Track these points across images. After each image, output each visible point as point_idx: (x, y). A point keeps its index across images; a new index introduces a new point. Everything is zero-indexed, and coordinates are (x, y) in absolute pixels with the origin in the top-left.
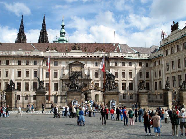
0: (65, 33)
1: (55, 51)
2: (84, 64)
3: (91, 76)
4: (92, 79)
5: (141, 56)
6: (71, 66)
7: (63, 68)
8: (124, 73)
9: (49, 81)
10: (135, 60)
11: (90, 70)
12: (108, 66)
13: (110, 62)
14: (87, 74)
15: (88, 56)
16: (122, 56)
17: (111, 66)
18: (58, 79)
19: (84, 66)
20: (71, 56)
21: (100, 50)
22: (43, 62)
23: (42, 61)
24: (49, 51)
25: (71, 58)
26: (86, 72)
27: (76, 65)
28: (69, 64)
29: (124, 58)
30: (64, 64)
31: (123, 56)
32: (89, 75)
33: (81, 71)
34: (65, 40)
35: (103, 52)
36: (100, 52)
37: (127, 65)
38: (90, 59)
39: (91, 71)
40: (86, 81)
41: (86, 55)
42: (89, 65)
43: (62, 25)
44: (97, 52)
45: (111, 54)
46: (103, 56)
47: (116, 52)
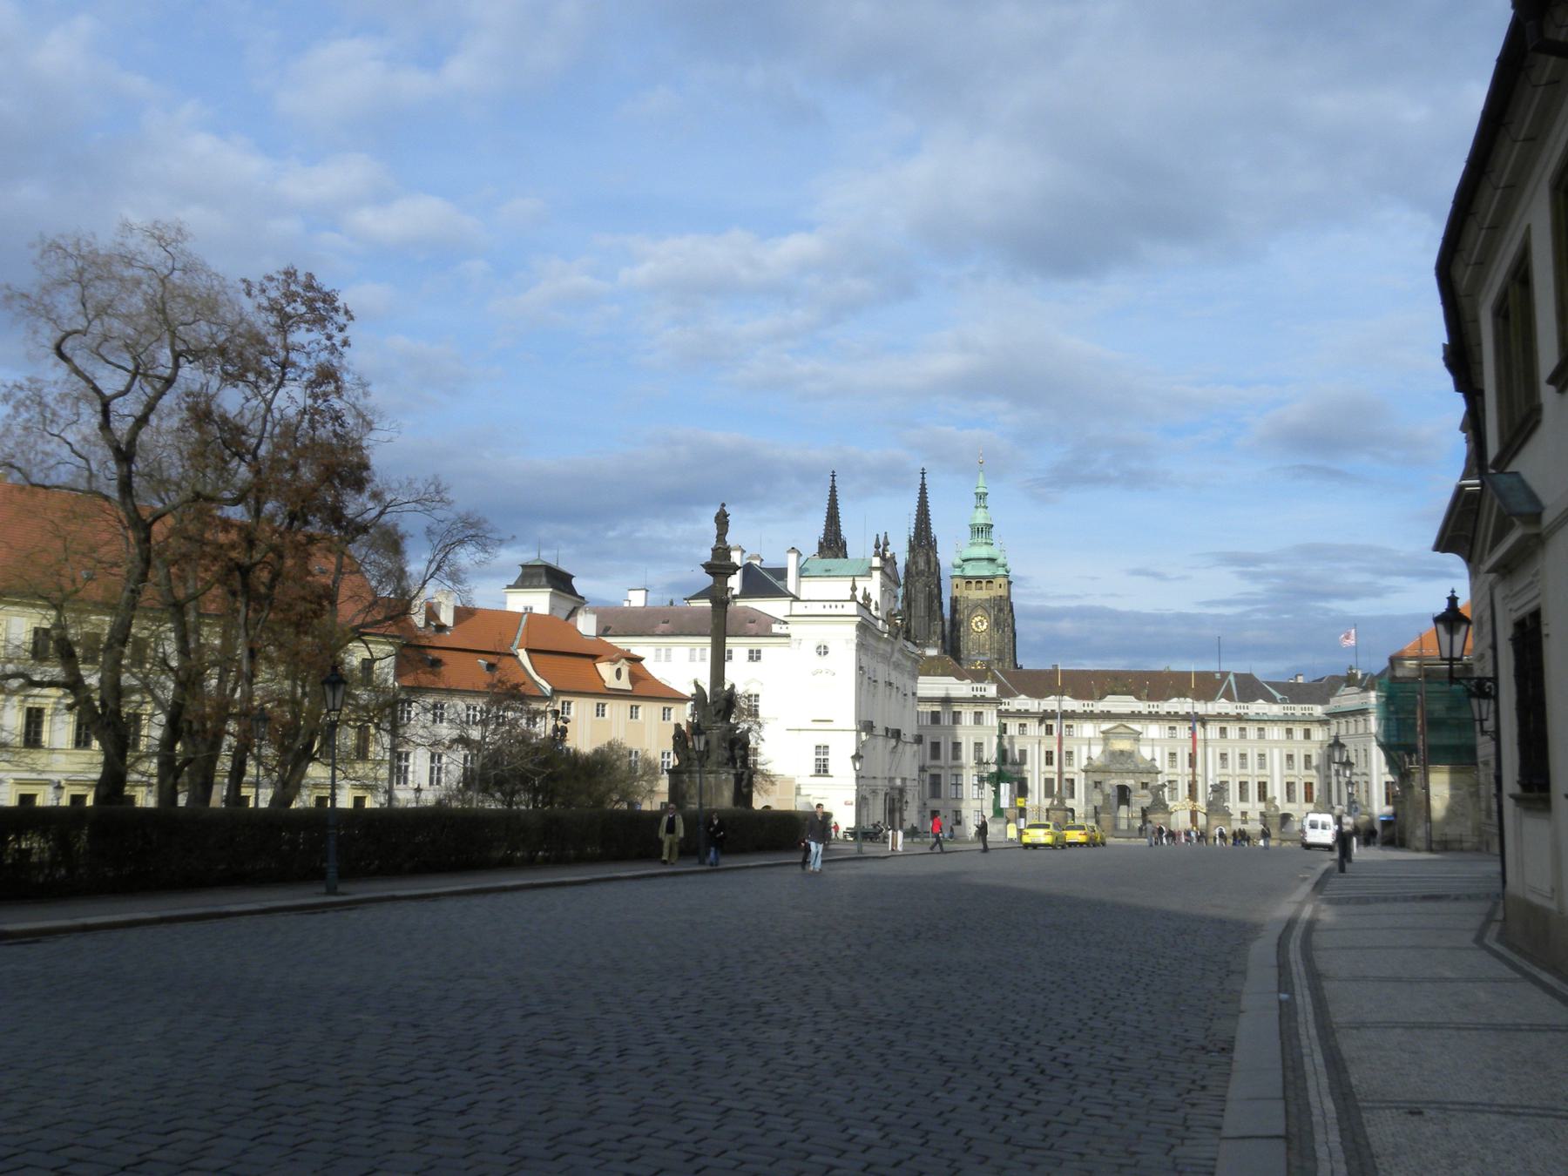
3: (1158, 764)
6: (1106, 734)
7: (1089, 742)
8: (1243, 756)
9: (1061, 773)
10: (1274, 721)
11: (1156, 744)
13: (1208, 727)
14: (1148, 758)
18: (1076, 769)
21: (1181, 694)
25: (1107, 716)
26: (1146, 752)
27: (1119, 736)
30: (1088, 729)
31: (1242, 711)
34: (992, 560)
37: (1252, 732)
38: (1154, 717)
42: (1154, 730)
43: (981, 490)
45: (1210, 705)
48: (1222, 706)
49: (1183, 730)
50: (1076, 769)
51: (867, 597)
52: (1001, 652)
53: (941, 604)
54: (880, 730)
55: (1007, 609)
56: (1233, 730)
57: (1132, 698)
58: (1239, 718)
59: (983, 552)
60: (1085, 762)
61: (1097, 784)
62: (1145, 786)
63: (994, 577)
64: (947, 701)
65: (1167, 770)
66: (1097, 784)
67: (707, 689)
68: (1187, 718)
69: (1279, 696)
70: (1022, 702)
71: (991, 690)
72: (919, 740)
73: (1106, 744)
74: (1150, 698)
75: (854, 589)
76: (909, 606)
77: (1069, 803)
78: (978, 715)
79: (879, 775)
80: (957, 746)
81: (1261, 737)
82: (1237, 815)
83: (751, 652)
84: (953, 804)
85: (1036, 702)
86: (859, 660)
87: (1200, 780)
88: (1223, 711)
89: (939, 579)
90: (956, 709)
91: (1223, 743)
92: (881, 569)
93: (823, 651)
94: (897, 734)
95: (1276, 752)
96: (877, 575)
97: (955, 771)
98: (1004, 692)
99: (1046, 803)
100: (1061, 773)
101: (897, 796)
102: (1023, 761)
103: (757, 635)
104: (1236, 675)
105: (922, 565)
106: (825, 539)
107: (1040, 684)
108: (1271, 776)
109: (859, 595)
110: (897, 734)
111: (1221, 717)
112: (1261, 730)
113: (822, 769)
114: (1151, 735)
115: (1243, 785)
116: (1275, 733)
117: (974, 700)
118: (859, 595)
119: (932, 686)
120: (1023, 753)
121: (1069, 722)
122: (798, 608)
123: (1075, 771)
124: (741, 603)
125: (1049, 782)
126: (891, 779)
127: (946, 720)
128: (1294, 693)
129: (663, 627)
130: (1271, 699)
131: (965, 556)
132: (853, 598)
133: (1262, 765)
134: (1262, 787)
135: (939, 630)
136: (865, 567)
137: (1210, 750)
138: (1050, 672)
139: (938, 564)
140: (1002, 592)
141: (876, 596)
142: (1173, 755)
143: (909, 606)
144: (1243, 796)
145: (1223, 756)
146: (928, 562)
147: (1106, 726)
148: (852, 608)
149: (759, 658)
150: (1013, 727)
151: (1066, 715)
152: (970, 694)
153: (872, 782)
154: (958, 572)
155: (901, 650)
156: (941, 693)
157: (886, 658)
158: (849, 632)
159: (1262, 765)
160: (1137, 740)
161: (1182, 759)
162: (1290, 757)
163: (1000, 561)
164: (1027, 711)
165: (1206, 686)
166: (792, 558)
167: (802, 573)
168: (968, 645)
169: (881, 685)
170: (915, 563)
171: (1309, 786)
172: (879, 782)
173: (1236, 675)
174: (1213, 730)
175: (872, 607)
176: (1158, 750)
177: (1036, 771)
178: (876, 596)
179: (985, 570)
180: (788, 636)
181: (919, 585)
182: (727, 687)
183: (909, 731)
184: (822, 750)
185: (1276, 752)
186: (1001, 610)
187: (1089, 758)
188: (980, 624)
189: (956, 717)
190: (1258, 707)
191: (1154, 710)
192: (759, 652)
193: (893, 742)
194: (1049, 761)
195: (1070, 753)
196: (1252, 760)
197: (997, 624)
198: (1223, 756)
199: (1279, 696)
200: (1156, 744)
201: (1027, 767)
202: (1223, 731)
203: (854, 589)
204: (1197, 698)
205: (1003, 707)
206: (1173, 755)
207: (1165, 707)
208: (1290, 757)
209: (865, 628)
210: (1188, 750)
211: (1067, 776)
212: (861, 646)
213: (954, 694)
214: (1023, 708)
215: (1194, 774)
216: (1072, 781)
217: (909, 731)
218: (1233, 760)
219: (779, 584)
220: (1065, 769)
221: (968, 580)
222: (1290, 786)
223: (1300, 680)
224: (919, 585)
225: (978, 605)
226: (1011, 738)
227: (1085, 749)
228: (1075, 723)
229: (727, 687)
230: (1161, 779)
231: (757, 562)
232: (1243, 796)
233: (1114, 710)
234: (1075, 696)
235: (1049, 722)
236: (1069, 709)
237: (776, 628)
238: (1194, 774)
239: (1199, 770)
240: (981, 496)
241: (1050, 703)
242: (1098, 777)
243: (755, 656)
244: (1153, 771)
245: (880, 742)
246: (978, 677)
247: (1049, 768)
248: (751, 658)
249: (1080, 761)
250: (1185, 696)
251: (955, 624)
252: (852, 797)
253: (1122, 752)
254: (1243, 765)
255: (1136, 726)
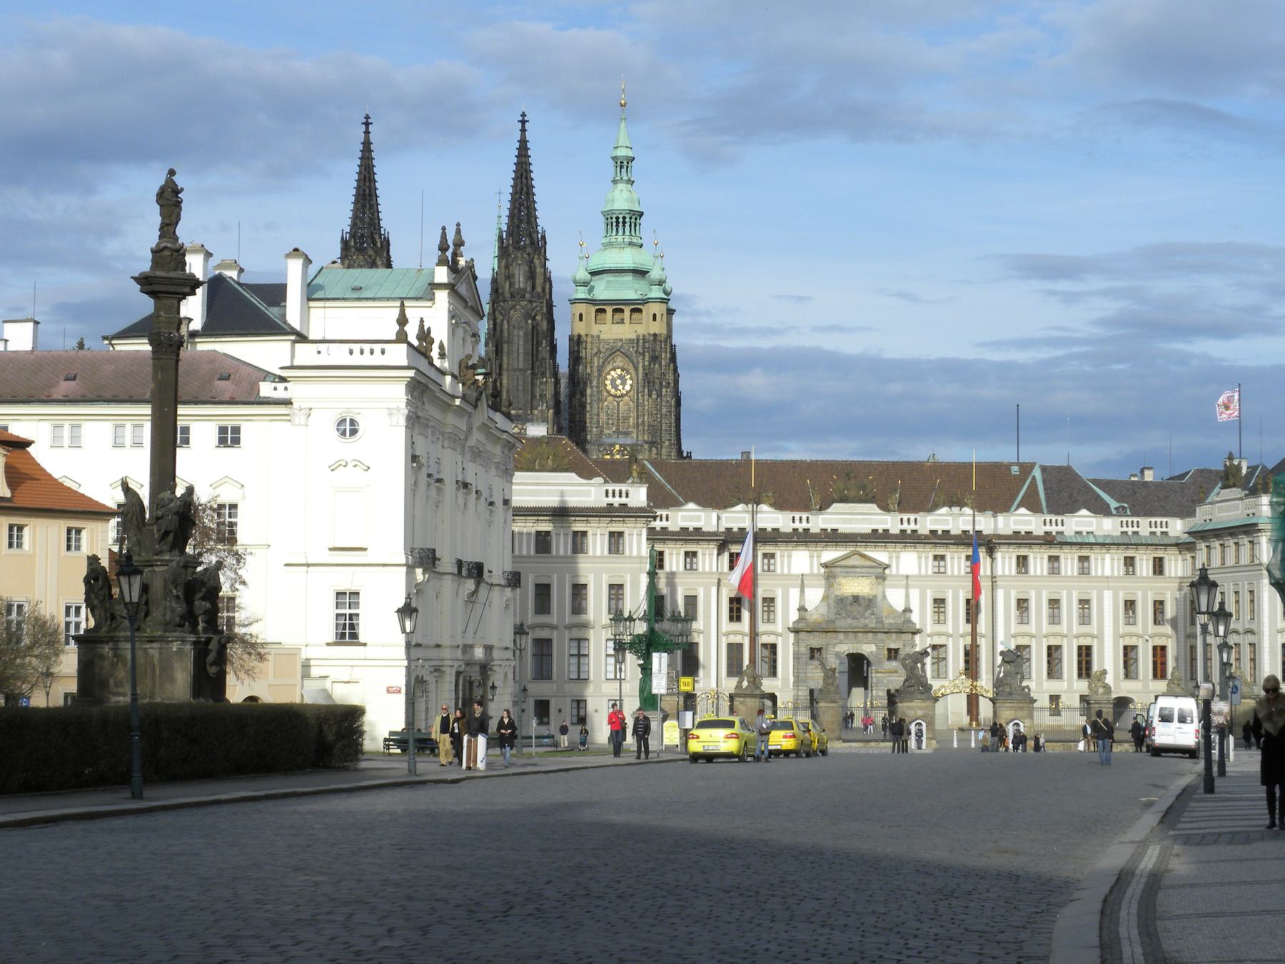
0: (641, 214)
1: (764, 507)
2: (888, 566)
3: (915, 617)
4: (919, 632)
5: (1135, 529)
7: (802, 582)
8: (1054, 603)
9: (754, 635)
10: (1105, 545)
12: (989, 573)
13: (998, 555)
15: (905, 526)
16: (1048, 528)
17: (999, 572)
18: (779, 626)
19: (887, 571)
20: (829, 527)
21: (955, 501)
22: (719, 554)
23: (715, 552)
24: (740, 507)
25: (832, 538)
26: (895, 598)
27: (851, 571)
28: (826, 566)
29: (1059, 539)
30: (800, 561)
31: (1054, 529)
32: (908, 610)
33: (874, 592)
34: (640, 273)
35: (968, 510)
36: (956, 510)
38: (909, 539)
39: (915, 594)
40: (894, 636)
41: (891, 522)
42: (909, 561)
43: (622, 152)
44: (944, 510)
45: (1001, 518)
46: (969, 528)
47: (1023, 510)
48: (1021, 520)
49: (957, 561)
50: (779, 626)
51: (425, 335)
52: (654, 431)
53: (553, 349)
54: (447, 564)
55: (665, 357)
56: (1038, 561)
57: (873, 507)
58: (1049, 540)
59: (626, 258)
60: (794, 616)
61: (814, 652)
62: (893, 654)
63: (645, 301)
64: (561, 513)
65: (929, 627)
66: (814, 652)
67: (145, 495)
68: (964, 540)
69: (1113, 504)
70: (689, 516)
71: (638, 496)
72: (514, 580)
73: (829, 586)
74: (903, 507)
75: (402, 321)
76: (498, 351)
77: (768, 685)
78: (616, 537)
79: (446, 642)
80: (579, 590)
81: (1084, 571)
82: (1043, 701)
83: (223, 430)
84: (572, 688)
85: (714, 514)
86: (411, 443)
87: (983, 644)
88: (1023, 529)
89: (550, 306)
90: (578, 527)
91: (1022, 582)
92: (451, 287)
93: (348, 428)
94: (477, 571)
95: (1108, 595)
96: (442, 296)
97: (576, 633)
98: (660, 499)
99: (730, 685)
100: (754, 635)
101: (475, 675)
102: (691, 616)
103: (233, 402)
104: (1044, 469)
105: (521, 280)
106: (353, 234)
107: (721, 484)
108: (1100, 636)
109: (412, 331)
110: (477, 571)
111: (1020, 539)
112: (1084, 559)
113: (348, 632)
114: (903, 571)
115: (1053, 651)
116: (1107, 564)
117: (609, 512)
118: (412, 331)
119: (536, 489)
120: (691, 601)
121: (769, 549)
122: (305, 354)
123: (777, 630)
124: (204, 346)
125: (735, 650)
126: (468, 648)
127: (561, 546)
128: (1139, 498)
129: (65, 387)
130: (1100, 509)
131: (596, 264)
132: (401, 338)
133: (1085, 619)
134: (1085, 654)
135: (549, 392)
136: (422, 282)
137: (1000, 594)
138: (738, 463)
139: (548, 280)
140: (658, 328)
141: (440, 333)
142: (939, 602)
143: (498, 351)
144: (1054, 670)
145: (1022, 604)
146: (531, 276)
147: (830, 554)
148: (399, 354)
149: (236, 441)
150: (674, 558)
151: (763, 537)
152: (602, 502)
153: (433, 653)
154: (582, 293)
155: (484, 427)
156: (552, 501)
157: (457, 441)
158: (396, 394)
159: (1085, 619)
160: (881, 578)
161: (955, 609)
162: (1130, 605)
163: (655, 274)
164: (697, 530)
165: (995, 486)
166: (295, 266)
167: (312, 293)
168: (599, 416)
169: (449, 486)
170: (509, 277)
171: (1160, 652)
172: (446, 653)
173: (1044, 469)
174: (1005, 561)
175: (435, 353)
176: (915, 594)
177: (713, 633)
178: (440, 333)
179: (628, 290)
180: (288, 403)
181: (516, 315)
182: (179, 492)
183: (498, 566)
184: (348, 598)
185: (1108, 595)
186: (655, 359)
187: (802, 609)
188: (618, 384)
189: (578, 542)
190: (1081, 522)
191: (909, 528)
192: (236, 430)
193: (470, 585)
194: (735, 616)
195: (769, 601)
196: (1070, 610)
197: (649, 382)
198: (1022, 604)
199: (1113, 504)
200: (912, 584)
201: (698, 625)
202: (1022, 561)
203: (402, 321)
204: (980, 507)
205: (657, 524)
206: (939, 602)
207: (927, 523)
208: (1130, 605)
209: (421, 389)
210: (964, 593)
211: (764, 639)
212: (415, 421)
213: (573, 501)
214: (691, 525)
215: (974, 634)
216: (773, 648)
217: (498, 566)
218: (1038, 609)
219: (272, 312)
220: (762, 627)
221: (600, 307)
222: (1129, 651)
223: (1149, 476)
224: (516, 315)
225: (615, 350)
226: (672, 576)
227: (794, 593)
228: (779, 551)
229: (179, 492)
230: (920, 643)
231: (232, 274)
232: (1054, 670)
233: (844, 528)
234: (779, 505)
235: (735, 549)
236: (769, 526)
237: (266, 389)
238: (974, 634)
239: (983, 626)
240: (623, 164)
241: (737, 517)
242: (816, 641)
243: (229, 437)
244: (907, 629)
245: (448, 584)
246: (616, 473)
247: (735, 626)
248: (222, 442)
249: (786, 613)
250: (961, 504)
251: (577, 383)
252: (400, 679)
253: (856, 599)
254: (1054, 619)
255: (880, 555)
